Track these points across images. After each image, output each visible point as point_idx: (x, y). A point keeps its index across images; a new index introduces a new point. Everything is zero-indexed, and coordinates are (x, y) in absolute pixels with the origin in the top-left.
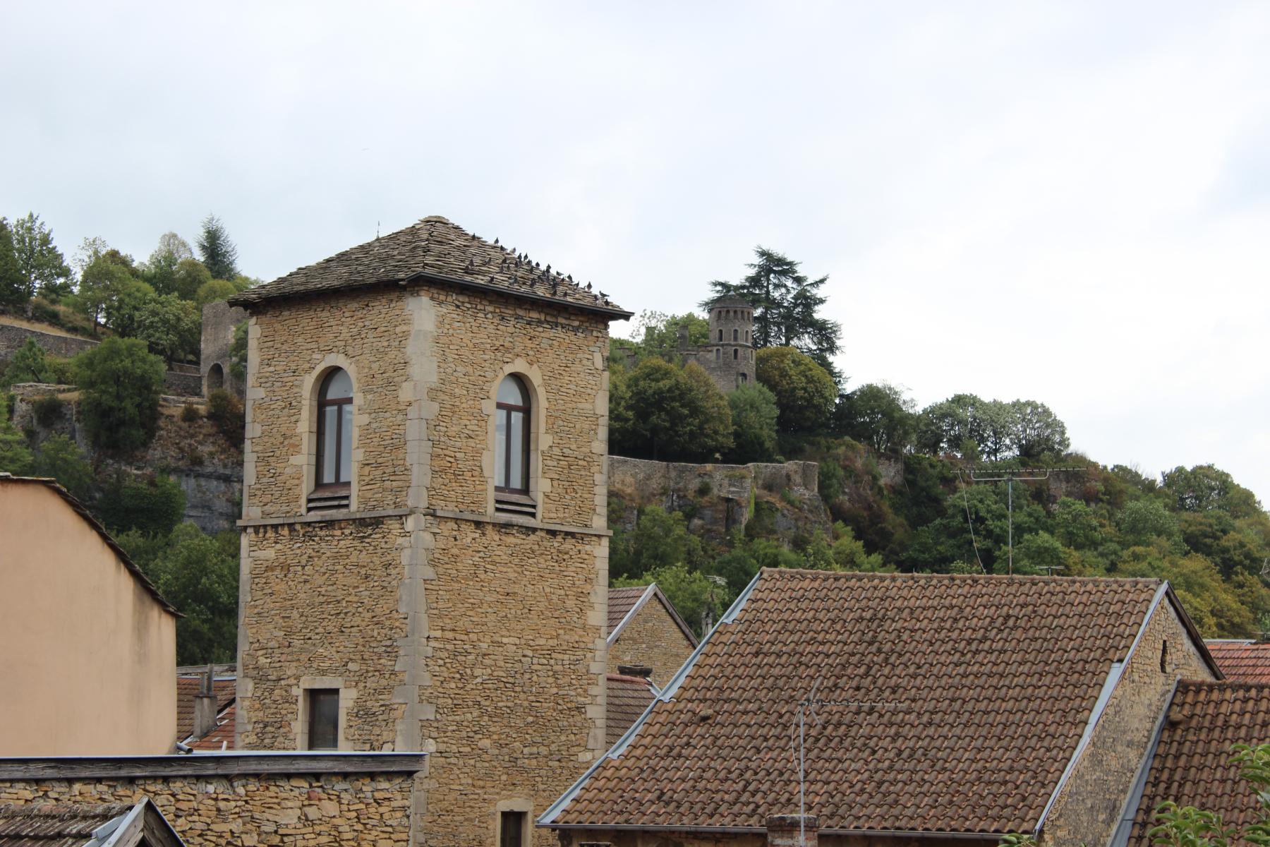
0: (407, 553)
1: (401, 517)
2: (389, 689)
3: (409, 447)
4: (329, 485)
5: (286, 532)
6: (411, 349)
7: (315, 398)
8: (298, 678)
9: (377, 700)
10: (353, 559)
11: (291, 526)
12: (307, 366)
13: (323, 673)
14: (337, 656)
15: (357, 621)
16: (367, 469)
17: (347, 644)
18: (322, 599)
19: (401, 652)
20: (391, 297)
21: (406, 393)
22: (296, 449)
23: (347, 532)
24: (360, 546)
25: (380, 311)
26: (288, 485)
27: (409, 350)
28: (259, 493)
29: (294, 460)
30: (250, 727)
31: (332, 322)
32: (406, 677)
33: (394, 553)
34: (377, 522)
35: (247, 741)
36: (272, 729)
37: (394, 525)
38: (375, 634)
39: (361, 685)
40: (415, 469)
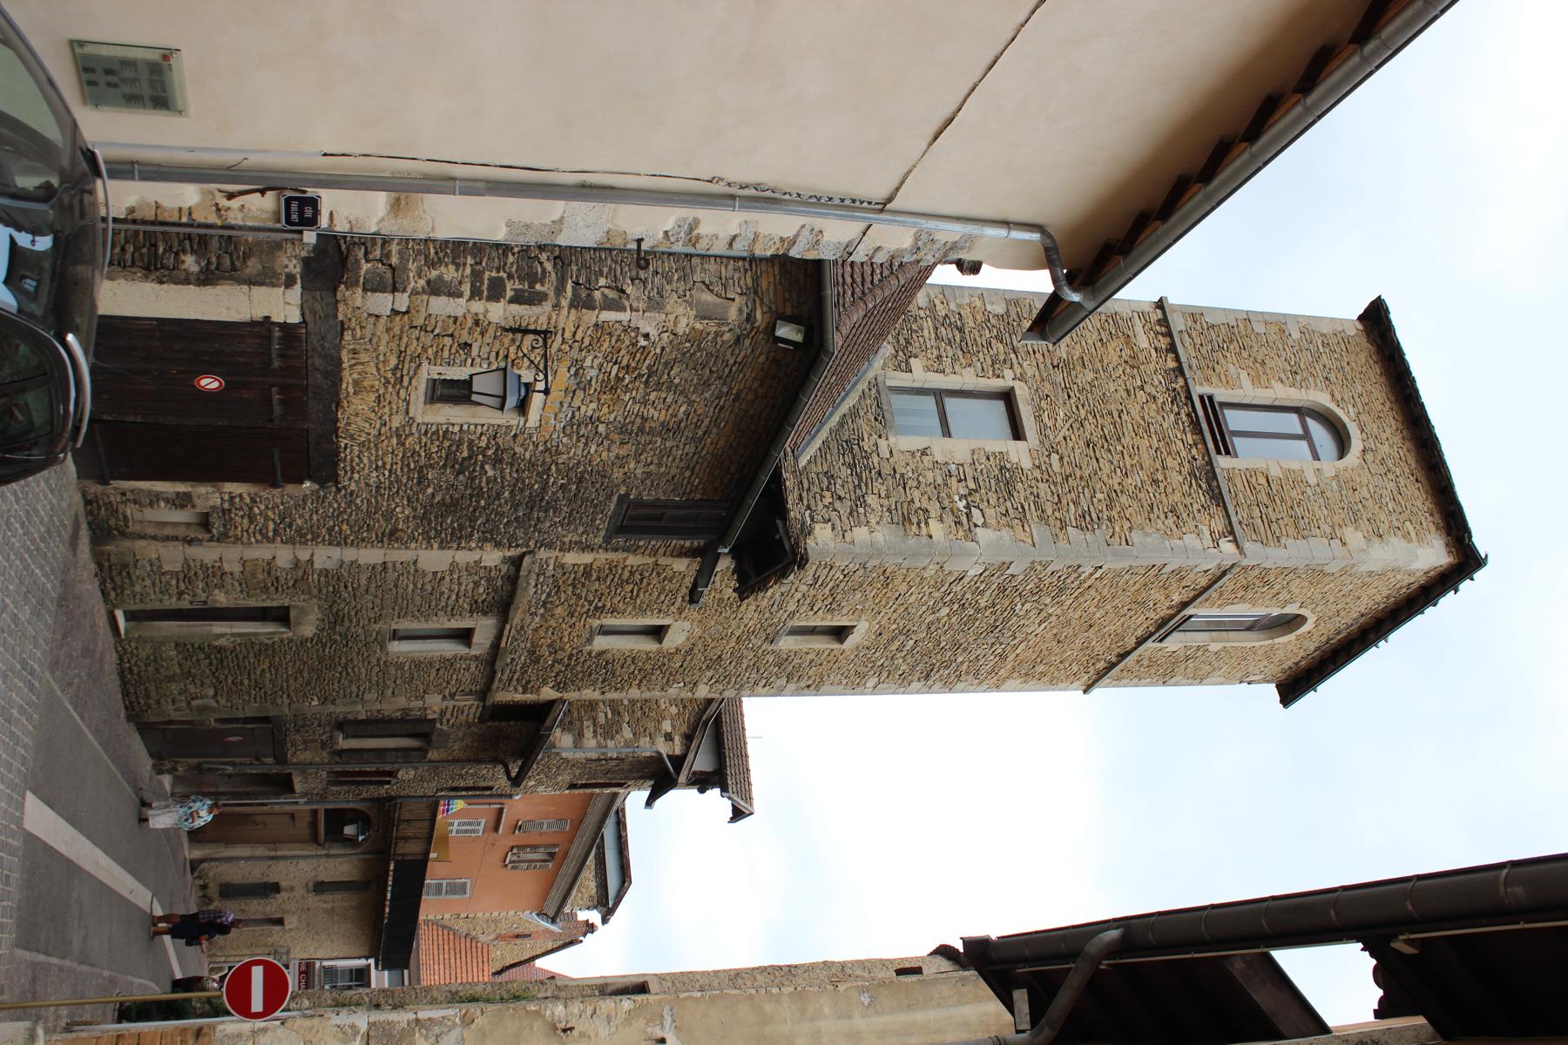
0: (1197, 544)
1: (1232, 532)
2: (1043, 518)
3: (1301, 542)
4: (37, 288)
5: (1172, 364)
6: (1396, 542)
7: (1306, 405)
8: (1022, 378)
9: (1026, 498)
10: (1170, 462)
11: (1180, 371)
12: (1338, 396)
13: (1038, 418)
14: (1060, 438)
15: (1106, 469)
16: (1262, 481)
17: (1077, 451)
18: (1116, 414)
19: (1089, 536)
20: (1437, 516)
21: (1354, 537)
22: (1255, 380)
23: (1194, 451)
24: (1185, 471)
25: (1418, 499)
26: (1218, 368)
27: (1394, 540)
28: (1198, 327)
29: (1245, 381)
30: (953, 307)
31: (1388, 431)
32: (1062, 544)
33: (1192, 524)
34: (1217, 497)
35: (937, 302)
36: (958, 338)
37: (1219, 524)
38: (1099, 496)
39: (1037, 474)
40: (1282, 552)
